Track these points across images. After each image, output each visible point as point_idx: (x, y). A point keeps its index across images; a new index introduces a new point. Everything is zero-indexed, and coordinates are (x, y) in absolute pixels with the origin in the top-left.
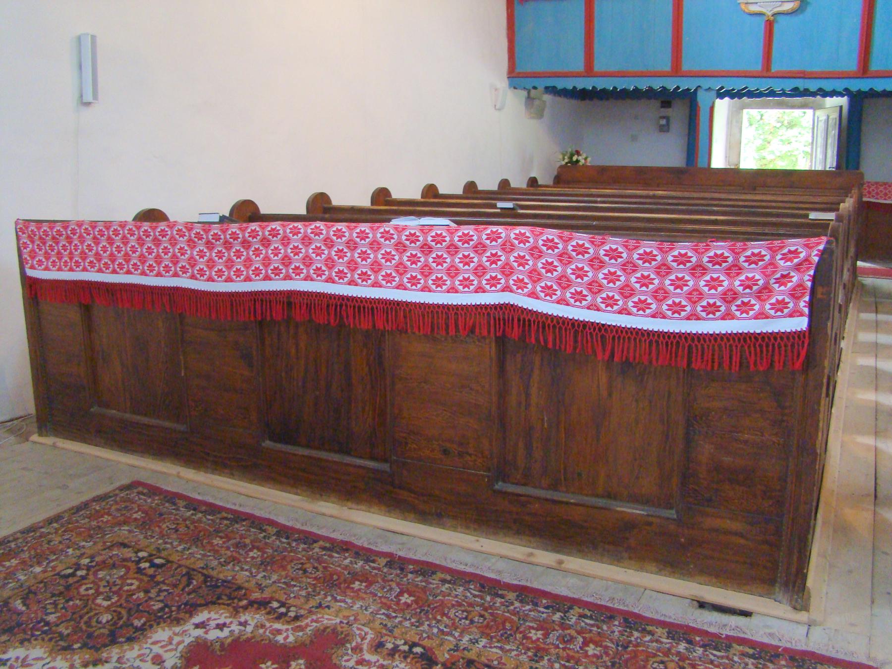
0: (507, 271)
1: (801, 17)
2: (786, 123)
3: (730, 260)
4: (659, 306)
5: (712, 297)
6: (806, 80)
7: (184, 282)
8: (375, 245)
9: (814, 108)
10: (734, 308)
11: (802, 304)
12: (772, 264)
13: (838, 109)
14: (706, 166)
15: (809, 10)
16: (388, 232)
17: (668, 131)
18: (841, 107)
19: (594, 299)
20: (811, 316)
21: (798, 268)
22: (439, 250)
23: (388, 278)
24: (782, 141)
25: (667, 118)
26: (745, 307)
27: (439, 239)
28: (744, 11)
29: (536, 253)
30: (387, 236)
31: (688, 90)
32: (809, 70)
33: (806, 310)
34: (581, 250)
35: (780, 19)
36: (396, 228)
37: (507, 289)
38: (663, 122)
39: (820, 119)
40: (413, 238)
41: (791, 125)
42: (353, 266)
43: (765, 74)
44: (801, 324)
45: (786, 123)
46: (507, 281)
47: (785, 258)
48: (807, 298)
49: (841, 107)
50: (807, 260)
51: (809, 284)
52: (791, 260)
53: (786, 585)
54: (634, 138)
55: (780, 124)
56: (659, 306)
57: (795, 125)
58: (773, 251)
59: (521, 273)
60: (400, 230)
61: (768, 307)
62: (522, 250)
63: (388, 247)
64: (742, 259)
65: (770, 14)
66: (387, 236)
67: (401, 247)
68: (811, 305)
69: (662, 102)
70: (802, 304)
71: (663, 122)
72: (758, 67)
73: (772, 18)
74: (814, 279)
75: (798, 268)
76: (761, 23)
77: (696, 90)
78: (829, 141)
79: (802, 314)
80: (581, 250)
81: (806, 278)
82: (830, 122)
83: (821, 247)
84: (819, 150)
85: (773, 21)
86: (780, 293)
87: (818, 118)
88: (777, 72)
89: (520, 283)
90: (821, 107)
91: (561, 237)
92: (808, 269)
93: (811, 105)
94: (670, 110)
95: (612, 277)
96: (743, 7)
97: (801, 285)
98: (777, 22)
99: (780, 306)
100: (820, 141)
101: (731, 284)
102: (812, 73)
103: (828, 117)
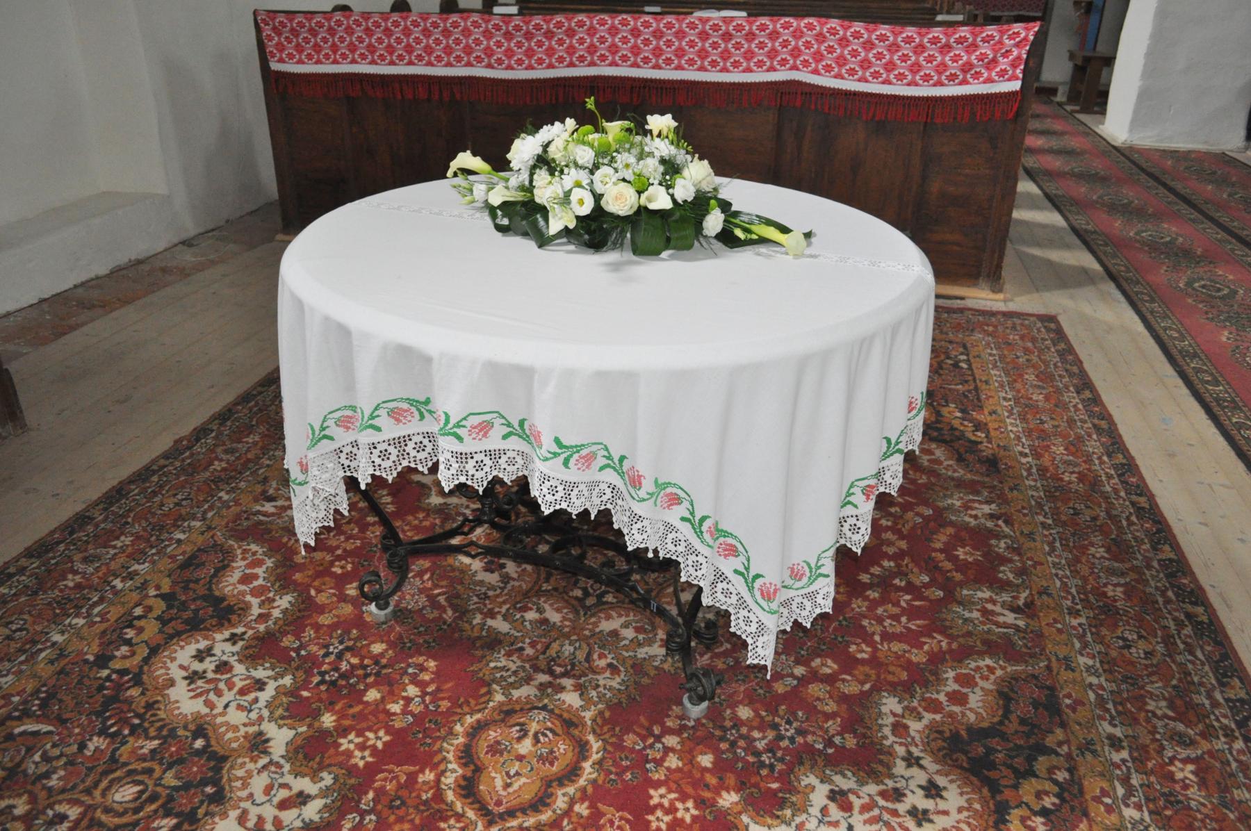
0: (796, 52)
3: (970, 40)
4: (914, 77)
5: (954, 68)
7: (480, 72)
8: (680, 34)
10: (969, 76)
12: (1000, 42)
16: (693, 23)
19: (864, 73)
20: (1023, 80)
21: (1017, 45)
22: (739, 38)
23: (691, 62)
26: (977, 75)
27: (739, 28)
29: (820, 38)
30: (692, 26)
34: (857, 35)
36: (700, 19)
37: (794, 68)
40: (716, 28)
42: (657, 52)
44: (1016, 85)
46: (795, 62)
47: (1010, 38)
48: (1022, 67)
50: (1025, 39)
51: (1025, 56)
52: (1014, 39)
53: (988, 276)
56: (914, 77)
58: (1002, 33)
59: (807, 55)
60: (704, 21)
61: (994, 74)
62: (809, 36)
63: (692, 35)
64: (979, 39)
66: (692, 26)
67: (704, 36)
68: (1024, 72)
70: (1018, 71)
74: (1029, 53)
75: (1017, 45)
79: (1017, 79)
80: (857, 35)
81: (1024, 52)
83: (1036, 29)
86: (1004, 63)
89: (806, 63)
91: (842, 26)
92: (1026, 45)
95: (879, 56)
97: (1019, 58)
99: (1002, 73)
101: (969, 58)
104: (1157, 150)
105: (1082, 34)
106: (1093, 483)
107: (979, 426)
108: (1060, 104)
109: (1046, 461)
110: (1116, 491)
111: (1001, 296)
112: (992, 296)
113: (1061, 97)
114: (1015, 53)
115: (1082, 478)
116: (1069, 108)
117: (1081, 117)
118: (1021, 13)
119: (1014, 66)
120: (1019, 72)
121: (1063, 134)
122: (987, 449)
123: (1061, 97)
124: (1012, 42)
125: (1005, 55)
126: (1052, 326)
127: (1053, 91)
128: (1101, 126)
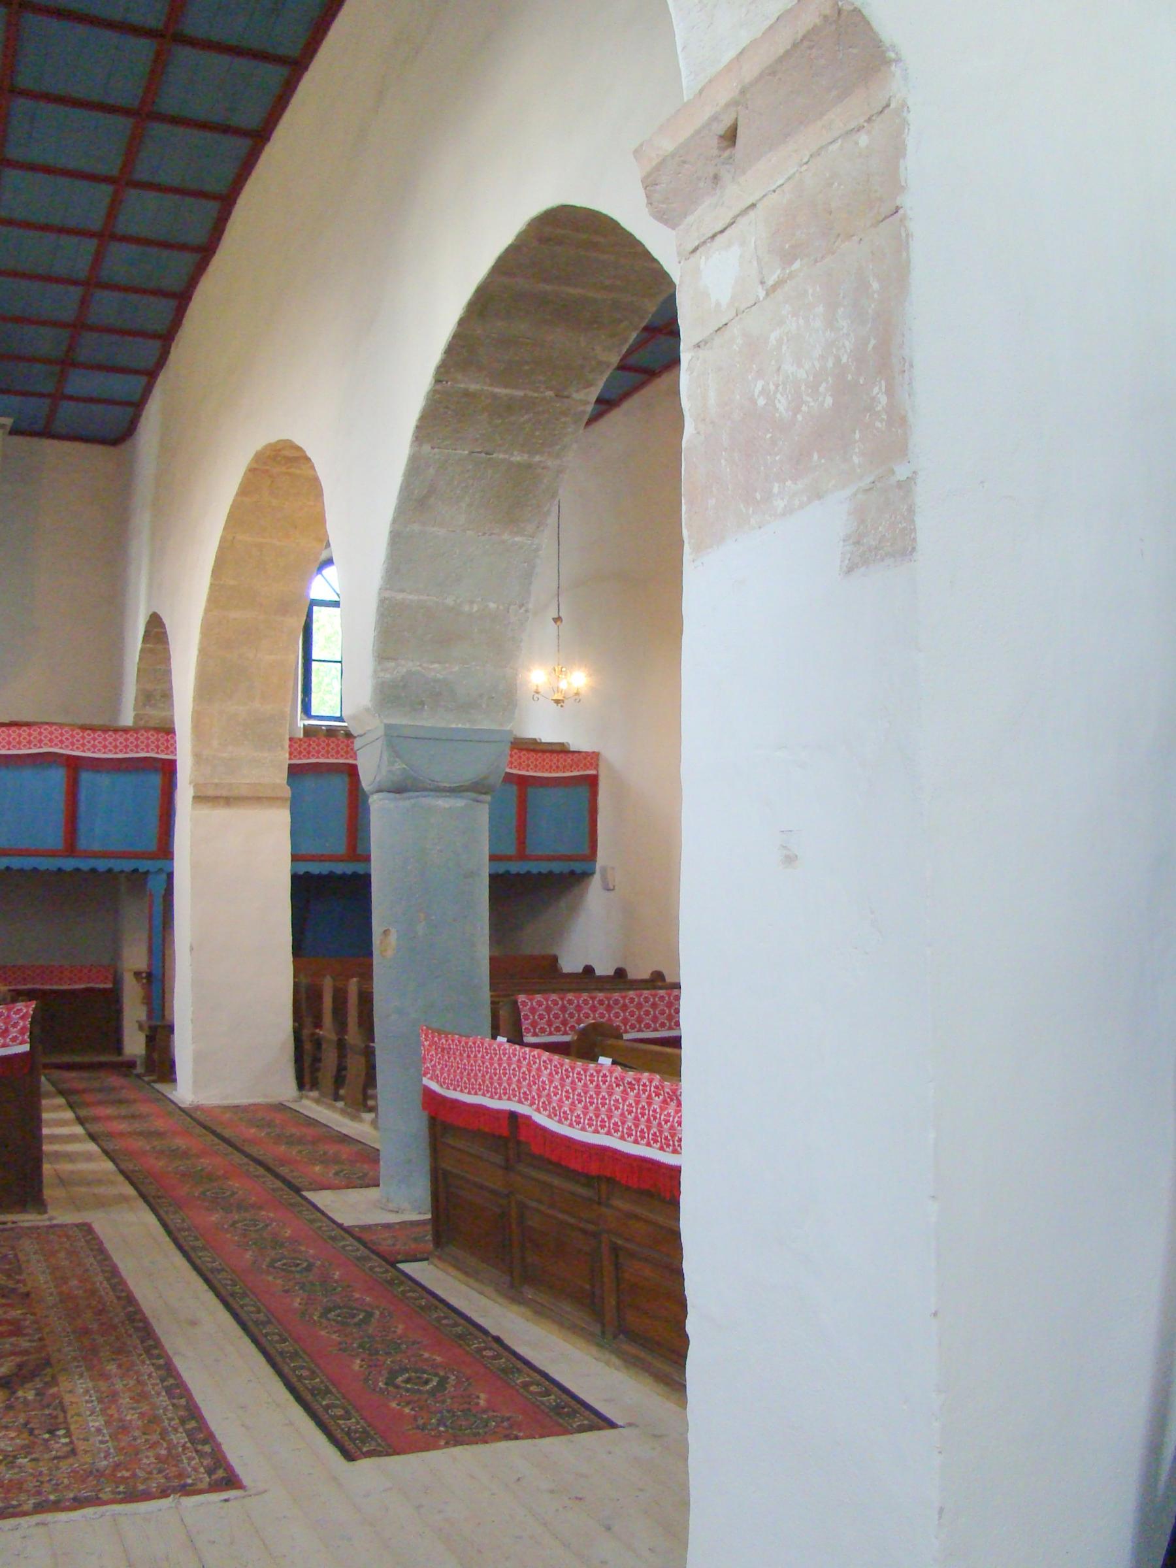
11: (26, 1037)
12: (9, 1017)
20: (31, 1042)
21: (22, 1018)
33: (28, 1040)
44: (26, 1048)
47: (16, 1013)
48: (28, 1034)
58: (9, 1010)
68: (31, 1036)
74: (31, 1023)
75: (22, 1018)
79: (26, 1042)
81: (27, 1023)
83: (34, 1006)
86: (14, 1032)
97: (23, 1028)
99: (14, 1039)
104: (219, 1107)
105: (148, 1000)
106: (93, 1292)
107: (18, 1282)
108: (139, 1076)
109: (64, 1288)
110: (107, 1293)
111: (46, 1216)
112: (39, 1217)
113: (140, 1070)
114: (21, 1024)
115: (85, 1291)
116: (146, 1079)
117: (158, 1086)
119: (23, 1034)
120: (26, 1037)
121: (134, 1101)
122: (22, 1289)
123: (140, 1070)
124: (18, 1016)
125: (15, 1025)
126: (85, 1228)
127: (131, 1065)
128: (174, 1092)
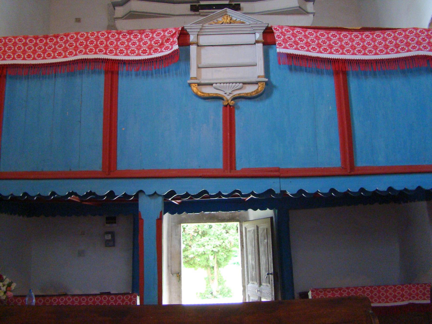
1: (267, 102)
2: (200, 233)
6: (282, 180)
9: (241, 220)
13: (269, 220)
14: (156, 303)
15: (276, 95)
17: (114, 245)
18: (272, 218)
24: (199, 245)
25: (112, 234)
28: (196, 95)
31: (126, 196)
32: (283, 166)
35: (241, 104)
38: (109, 237)
39: (248, 230)
41: (204, 234)
43: (229, 174)
45: (200, 233)
49: (272, 218)
54: (81, 254)
55: (196, 234)
57: (207, 234)
65: (229, 97)
69: (107, 219)
71: (109, 237)
72: (220, 165)
73: (232, 103)
76: (219, 105)
77: (137, 196)
78: (262, 249)
82: (260, 232)
84: (250, 257)
85: (233, 106)
87: (246, 229)
88: (243, 170)
90: (246, 220)
93: (237, 218)
94: (114, 225)
96: (195, 89)
98: (238, 108)
100: (250, 248)
102: (288, 170)
103: (258, 227)
118: (411, 301)
